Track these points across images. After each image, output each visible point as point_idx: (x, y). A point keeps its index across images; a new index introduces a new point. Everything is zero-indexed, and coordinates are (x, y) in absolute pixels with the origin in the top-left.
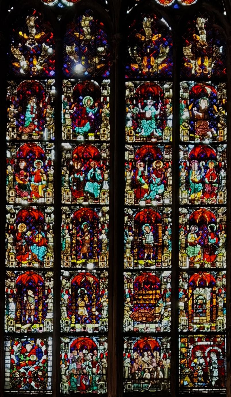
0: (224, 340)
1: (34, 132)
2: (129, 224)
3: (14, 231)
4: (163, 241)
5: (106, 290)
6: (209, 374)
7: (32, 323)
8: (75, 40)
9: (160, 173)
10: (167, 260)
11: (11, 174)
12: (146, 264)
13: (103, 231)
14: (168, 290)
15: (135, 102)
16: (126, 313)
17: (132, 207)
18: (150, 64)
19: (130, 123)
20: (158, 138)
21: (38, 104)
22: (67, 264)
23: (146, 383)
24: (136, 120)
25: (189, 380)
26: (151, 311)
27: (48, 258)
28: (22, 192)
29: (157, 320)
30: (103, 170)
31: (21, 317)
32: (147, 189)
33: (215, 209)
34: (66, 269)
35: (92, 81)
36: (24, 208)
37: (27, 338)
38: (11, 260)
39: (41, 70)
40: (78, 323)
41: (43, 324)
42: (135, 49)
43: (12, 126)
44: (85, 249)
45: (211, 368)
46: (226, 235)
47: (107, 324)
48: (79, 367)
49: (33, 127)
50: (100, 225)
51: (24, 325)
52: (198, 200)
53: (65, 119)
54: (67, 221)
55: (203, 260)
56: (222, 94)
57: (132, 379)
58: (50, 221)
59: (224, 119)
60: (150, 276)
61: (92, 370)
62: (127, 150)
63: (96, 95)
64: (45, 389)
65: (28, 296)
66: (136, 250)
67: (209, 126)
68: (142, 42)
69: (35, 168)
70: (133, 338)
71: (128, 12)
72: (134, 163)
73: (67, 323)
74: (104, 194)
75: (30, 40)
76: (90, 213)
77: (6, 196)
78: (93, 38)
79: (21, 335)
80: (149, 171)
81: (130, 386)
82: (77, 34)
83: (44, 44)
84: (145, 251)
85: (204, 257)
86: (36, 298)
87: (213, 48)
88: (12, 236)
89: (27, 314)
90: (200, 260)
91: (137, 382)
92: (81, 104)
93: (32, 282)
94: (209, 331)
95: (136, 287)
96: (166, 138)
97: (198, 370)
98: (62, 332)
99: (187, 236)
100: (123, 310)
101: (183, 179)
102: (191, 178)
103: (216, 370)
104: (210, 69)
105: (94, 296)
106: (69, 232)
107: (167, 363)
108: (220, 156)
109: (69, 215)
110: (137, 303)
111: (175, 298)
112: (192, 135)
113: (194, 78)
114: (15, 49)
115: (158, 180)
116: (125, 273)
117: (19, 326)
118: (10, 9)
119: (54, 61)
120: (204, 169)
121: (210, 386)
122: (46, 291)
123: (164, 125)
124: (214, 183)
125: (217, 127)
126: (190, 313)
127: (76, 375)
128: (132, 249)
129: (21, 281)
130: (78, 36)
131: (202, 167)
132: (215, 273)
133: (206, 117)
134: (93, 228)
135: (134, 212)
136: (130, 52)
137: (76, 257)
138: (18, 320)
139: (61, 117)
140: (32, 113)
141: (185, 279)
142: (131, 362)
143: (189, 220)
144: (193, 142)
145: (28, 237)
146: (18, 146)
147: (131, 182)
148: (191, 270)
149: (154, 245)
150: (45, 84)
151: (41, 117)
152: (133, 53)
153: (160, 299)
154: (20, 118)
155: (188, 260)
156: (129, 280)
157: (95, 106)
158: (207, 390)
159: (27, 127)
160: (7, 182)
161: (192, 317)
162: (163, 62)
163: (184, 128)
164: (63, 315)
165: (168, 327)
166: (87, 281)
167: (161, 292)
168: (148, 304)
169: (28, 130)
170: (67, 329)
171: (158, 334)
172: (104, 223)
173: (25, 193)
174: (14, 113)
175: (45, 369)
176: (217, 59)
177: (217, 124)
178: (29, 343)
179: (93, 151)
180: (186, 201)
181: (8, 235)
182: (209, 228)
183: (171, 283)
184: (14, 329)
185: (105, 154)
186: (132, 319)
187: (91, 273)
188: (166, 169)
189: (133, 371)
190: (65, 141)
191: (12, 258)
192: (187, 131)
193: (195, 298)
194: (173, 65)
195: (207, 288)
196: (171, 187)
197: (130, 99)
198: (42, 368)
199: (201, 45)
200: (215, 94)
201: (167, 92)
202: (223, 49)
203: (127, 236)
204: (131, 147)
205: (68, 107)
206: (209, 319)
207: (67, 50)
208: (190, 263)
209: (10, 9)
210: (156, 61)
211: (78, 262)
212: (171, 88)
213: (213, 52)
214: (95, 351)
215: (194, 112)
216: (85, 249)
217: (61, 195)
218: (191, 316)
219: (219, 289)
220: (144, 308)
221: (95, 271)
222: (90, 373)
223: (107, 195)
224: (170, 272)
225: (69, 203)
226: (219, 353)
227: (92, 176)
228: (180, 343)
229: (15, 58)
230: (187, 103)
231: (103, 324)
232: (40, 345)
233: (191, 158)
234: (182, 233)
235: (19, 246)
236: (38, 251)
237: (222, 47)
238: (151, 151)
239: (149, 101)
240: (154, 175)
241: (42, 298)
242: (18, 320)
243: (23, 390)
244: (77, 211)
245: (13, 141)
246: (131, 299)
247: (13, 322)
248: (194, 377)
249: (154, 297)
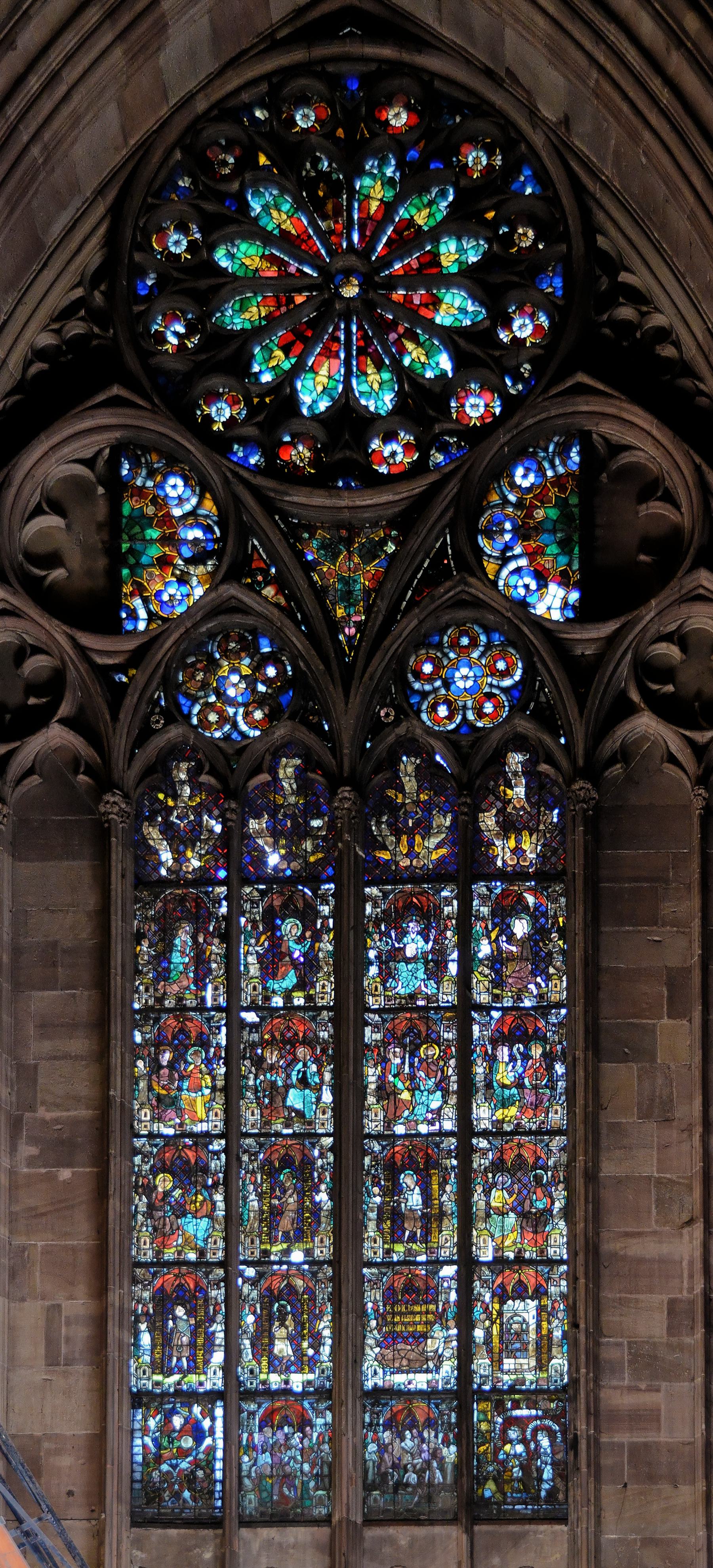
4: (441, 1204)
5: (329, 1304)
7: (185, 1373)
9: (434, 1068)
10: (448, 1244)
16: (368, 1351)
17: (378, 1137)
19: (373, 970)
21: (194, 938)
22: (252, 1253)
23: (410, 1494)
27: (215, 1243)
29: (431, 1364)
38: (143, 1247)
41: (205, 1373)
47: (330, 1372)
49: (185, 983)
50: (316, 1174)
52: (509, 1121)
53: (246, 965)
63: (307, 915)
65: (175, 1319)
66: (388, 1222)
73: (252, 1372)
74: (324, 1113)
80: (411, 1065)
83: (206, 817)
86: (193, 1322)
88: (145, 1199)
90: (514, 1243)
94: (533, 1387)
103: (549, 1467)
106: (255, 1190)
107: (450, 1453)
108: (554, 1032)
109: (256, 1154)
112: (496, 991)
114: (151, 829)
115: (431, 1083)
117: (158, 1378)
122: (211, 1308)
128: (380, 1220)
129: (162, 1289)
131: (518, 1056)
135: (384, 1148)
140: (183, 953)
141: (486, 1281)
143: (492, 1163)
150: (209, 897)
151: (200, 960)
153: (435, 1323)
155: (491, 1245)
156: (375, 1283)
157: (305, 938)
161: (501, 1362)
162: (438, 846)
163: (480, 978)
167: (437, 1308)
173: (171, 1113)
177: (547, 967)
180: (485, 1125)
186: (380, 1362)
189: (383, 1469)
190: (247, 1009)
192: (486, 983)
195: (528, 1301)
200: (543, 909)
201: (448, 905)
204: (377, 1018)
205: (253, 941)
206: (533, 1363)
208: (496, 1250)
211: (274, 1249)
212: (456, 898)
214: (308, 1428)
219: (555, 1301)
220: (405, 1340)
221: (306, 1267)
223: (329, 1113)
224: (455, 1267)
225: (257, 1131)
226: (555, 1432)
230: (486, 927)
232: (200, 1416)
234: (479, 1189)
239: (411, 925)
245: (146, 1011)
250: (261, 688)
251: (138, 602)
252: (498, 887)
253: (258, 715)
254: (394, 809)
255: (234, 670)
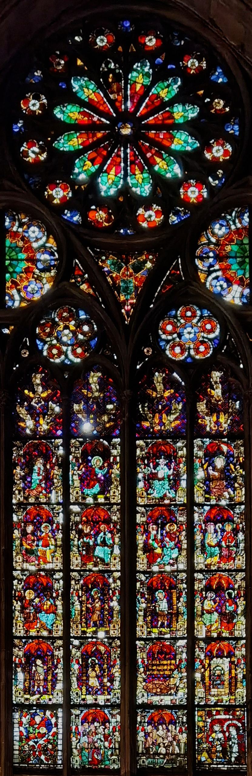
0: (244, 714)
1: (41, 494)
2: (141, 591)
3: (22, 598)
4: (178, 608)
5: (118, 660)
6: (229, 749)
7: (41, 694)
8: (83, 397)
9: (174, 536)
10: (182, 629)
11: (19, 538)
12: (160, 633)
13: (114, 598)
14: (184, 660)
15: (146, 462)
16: (139, 684)
17: (144, 573)
18: (162, 422)
19: (141, 485)
20: (171, 500)
21: (45, 465)
22: (77, 632)
23: (162, 758)
24: (148, 480)
25: (207, 756)
26: (165, 682)
27: (57, 627)
28: (29, 557)
29: (173, 691)
30: (114, 534)
31: (29, 687)
32: (160, 554)
33: (232, 574)
34: (76, 638)
35: (101, 440)
36: (32, 574)
37: (36, 710)
38: (18, 628)
39: (48, 430)
40: (89, 694)
41: (52, 695)
42: (146, 405)
43: (18, 488)
44: (95, 617)
45: (231, 743)
46: (245, 602)
47: (119, 695)
48: (90, 740)
49: (40, 489)
50: (111, 592)
51: (32, 696)
52: (214, 564)
53: (73, 481)
54: (76, 587)
55: (221, 628)
56: (239, 452)
57: (146, 754)
58: (58, 588)
59: (241, 479)
60: (164, 645)
61: (104, 744)
62: (139, 513)
63: (105, 455)
64: (55, 763)
65: (36, 665)
66: (150, 617)
67: (226, 486)
68: (153, 399)
69: (43, 532)
70: (147, 710)
71: (138, 367)
72: (146, 526)
73: (77, 694)
74: (115, 559)
75: (36, 399)
76: (100, 579)
77: (13, 561)
78: (101, 395)
79: (30, 707)
80: (162, 535)
81: (144, 761)
82: (85, 391)
83: (50, 403)
84: (159, 619)
85: (221, 626)
86: (45, 667)
87: (229, 403)
88: (19, 603)
89: (36, 684)
90: (217, 629)
91: (152, 757)
92: (90, 464)
93: (40, 651)
94: (227, 703)
95: (150, 657)
96: (180, 499)
97: (217, 745)
98: (72, 703)
99: (203, 603)
100: (136, 681)
101: (198, 543)
102: (207, 541)
103: (236, 745)
104: (226, 425)
105: (106, 666)
106: (78, 599)
107: (183, 738)
108: (238, 518)
109: (79, 580)
110: (151, 674)
111: (191, 668)
112: (207, 496)
113: (209, 435)
114: (21, 408)
115: (172, 544)
116: (137, 642)
117: (28, 696)
118: (15, 367)
119: (61, 420)
120: (221, 532)
121: (229, 762)
122: (55, 661)
123: (178, 486)
124: (231, 547)
125: (234, 487)
126: (207, 684)
127: (87, 749)
128: (145, 616)
129: (29, 651)
130: (86, 393)
131: (219, 530)
132: (234, 643)
133: (222, 476)
134: (103, 594)
135: (147, 578)
136: (141, 409)
137: (86, 625)
138: (27, 690)
139: (69, 478)
140: (39, 474)
141: (202, 648)
142: (145, 736)
143: (205, 586)
144: (208, 503)
145: (36, 604)
146: (25, 509)
147: (144, 546)
148: (208, 640)
149: (168, 613)
150: (52, 444)
151: (48, 479)
152: (144, 410)
153: (175, 669)
154: (26, 480)
155: (204, 629)
156: (142, 649)
157: (104, 467)
158: (226, 766)
159: (34, 489)
160: (14, 547)
161: (210, 689)
162: (176, 419)
163: (198, 489)
164: (73, 686)
165: (184, 700)
166: (97, 650)
167: (176, 662)
168: (163, 674)
169: (35, 492)
170: (77, 700)
171: (173, 707)
172: (115, 589)
173: (33, 558)
174: (20, 474)
175: (55, 743)
176: (234, 415)
177: (234, 484)
178: (38, 715)
179: (102, 514)
181: (15, 602)
182: (226, 595)
183: (186, 653)
184: (23, 700)
185: (116, 517)
186: (146, 690)
187: (102, 642)
188: (180, 532)
189: (147, 746)
190: (74, 504)
191: (20, 626)
192: (202, 492)
193: (212, 669)
194: (187, 422)
195: (225, 659)
196: (185, 551)
197: (141, 459)
198: (52, 741)
199: (216, 400)
200: (231, 453)
201: (181, 450)
202: (240, 403)
203: (139, 603)
204: (143, 509)
205: (76, 468)
206: (227, 691)
207: (74, 408)
208: (207, 632)
209: (15, 367)
210: (169, 418)
211: (88, 630)
212: (185, 446)
213: (229, 407)
214: (107, 724)
215: (209, 471)
216: (95, 617)
217: (70, 560)
218: (208, 688)
219: (238, 659)
220: (159, 678)
221: (106, 640)
222: (102, 747)
223: (118, 559)
224: (186, 641)
225: (79, 568)
226: (239, 727)
227: (102, 539)
228: (197, 717)
229: (21, 418)
230: (201, 462)
231: (115, 696)
232: (50, 717)
233: (207, 521)
234: (198, 600)
235: (27, 613)
236: (46, 619)
237: (238, 402)
238: (164, 513)
239: (161, 460)
240: (167, 539)
241: (51, 668)
242: (27, 690)
243: (32, 764)
244: (87, 576)
245: (20, 504)
246: (144, 670)
247: (22, 693)
248: (212, 753)
249: (169, 668)
250: (81, 337)
251: (14, 292)
252: (207, 441)
253: (79, 350)
254: (151, 400)
255: (66, 327)
